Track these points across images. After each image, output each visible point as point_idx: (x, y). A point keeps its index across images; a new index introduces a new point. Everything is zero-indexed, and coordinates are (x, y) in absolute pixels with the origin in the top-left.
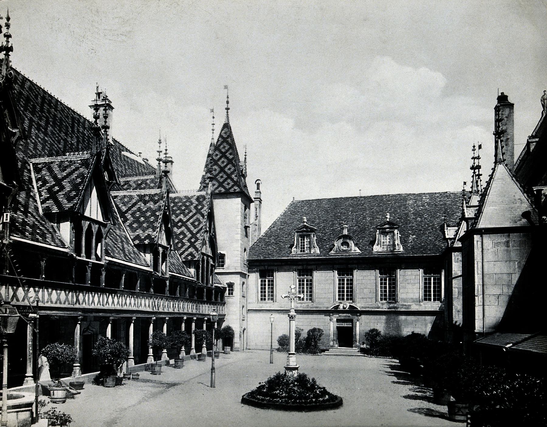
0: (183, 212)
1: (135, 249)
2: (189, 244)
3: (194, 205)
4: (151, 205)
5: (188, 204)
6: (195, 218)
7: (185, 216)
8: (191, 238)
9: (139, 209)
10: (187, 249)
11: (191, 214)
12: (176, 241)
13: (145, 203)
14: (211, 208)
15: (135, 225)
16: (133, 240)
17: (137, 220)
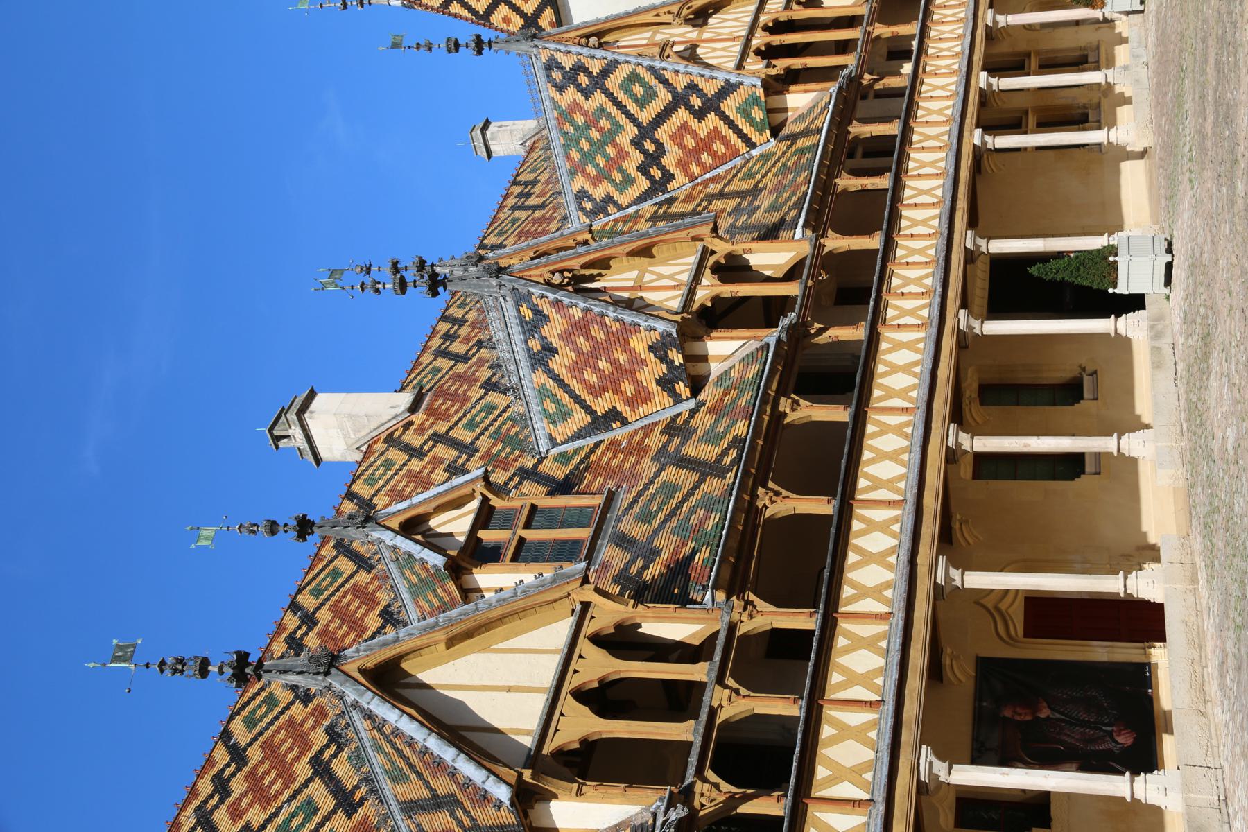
0: (610, 136)
2: (712, 118)
3: (579, 97)
4: (553, 331)
5: (580, 120)
6: (621, 95)
7: (618, 128)
8: (690, 108)
9: (576, 369)
10: (731, 124)
11: (613, 110)
12: (705, 157)
13: (550, 350)
15: (628, 389)
16: (678, 399)
17: (610, 383)
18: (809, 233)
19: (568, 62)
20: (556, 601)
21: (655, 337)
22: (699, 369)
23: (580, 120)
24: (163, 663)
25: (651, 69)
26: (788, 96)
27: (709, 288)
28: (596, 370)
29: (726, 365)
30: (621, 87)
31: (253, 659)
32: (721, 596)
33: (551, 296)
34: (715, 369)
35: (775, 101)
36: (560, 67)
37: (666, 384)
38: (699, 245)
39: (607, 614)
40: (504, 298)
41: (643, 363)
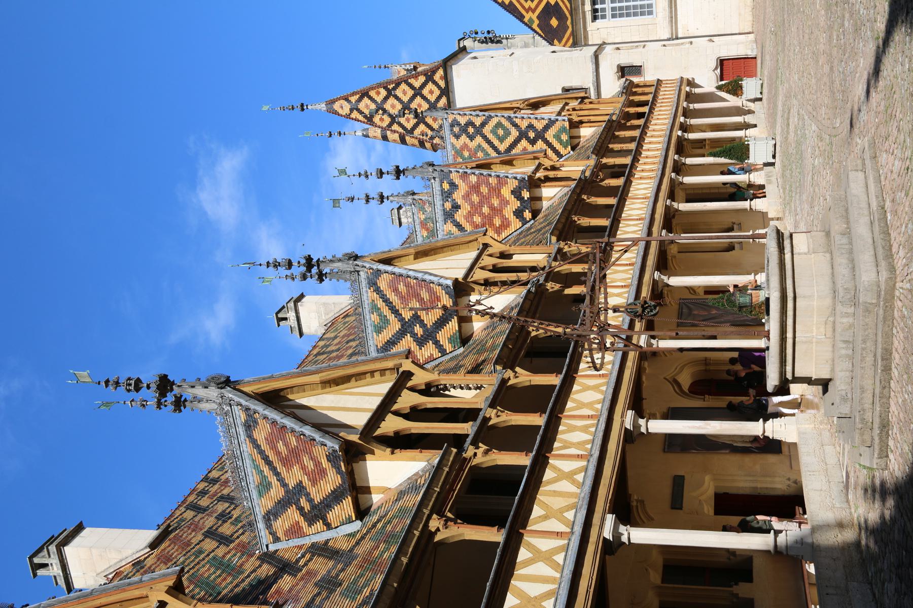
1: (540, 216)
4: (458, 196)
5: (466, 154)
6: (491, 137)
8: (528, 139)
9: (469, 216)
10: (550, 145)
11: (485, 145)
13: (456, 207)
14: (474, 109)
15: (497, 222)
18: (594, 156)
19: (463, 121)
20: (470, 242)
21: (516, 183)
22: (537, 205)
23: (466, 154)
24: (268, 263)
25: (509, 119)
26: (582, 129)
27: (540, 174)
28: (481, 214)
29: (550, 203)
30: (491, 132)
31: (315, 260)
32: (554, 239)
33: (461, 171)
34: (545, 204)
35: (574, 132)
36: (459, 124)
37: (518, 213)
38: (537, 162)
39: (496, 248)
40: (434, 178)
41: (508, 202)
